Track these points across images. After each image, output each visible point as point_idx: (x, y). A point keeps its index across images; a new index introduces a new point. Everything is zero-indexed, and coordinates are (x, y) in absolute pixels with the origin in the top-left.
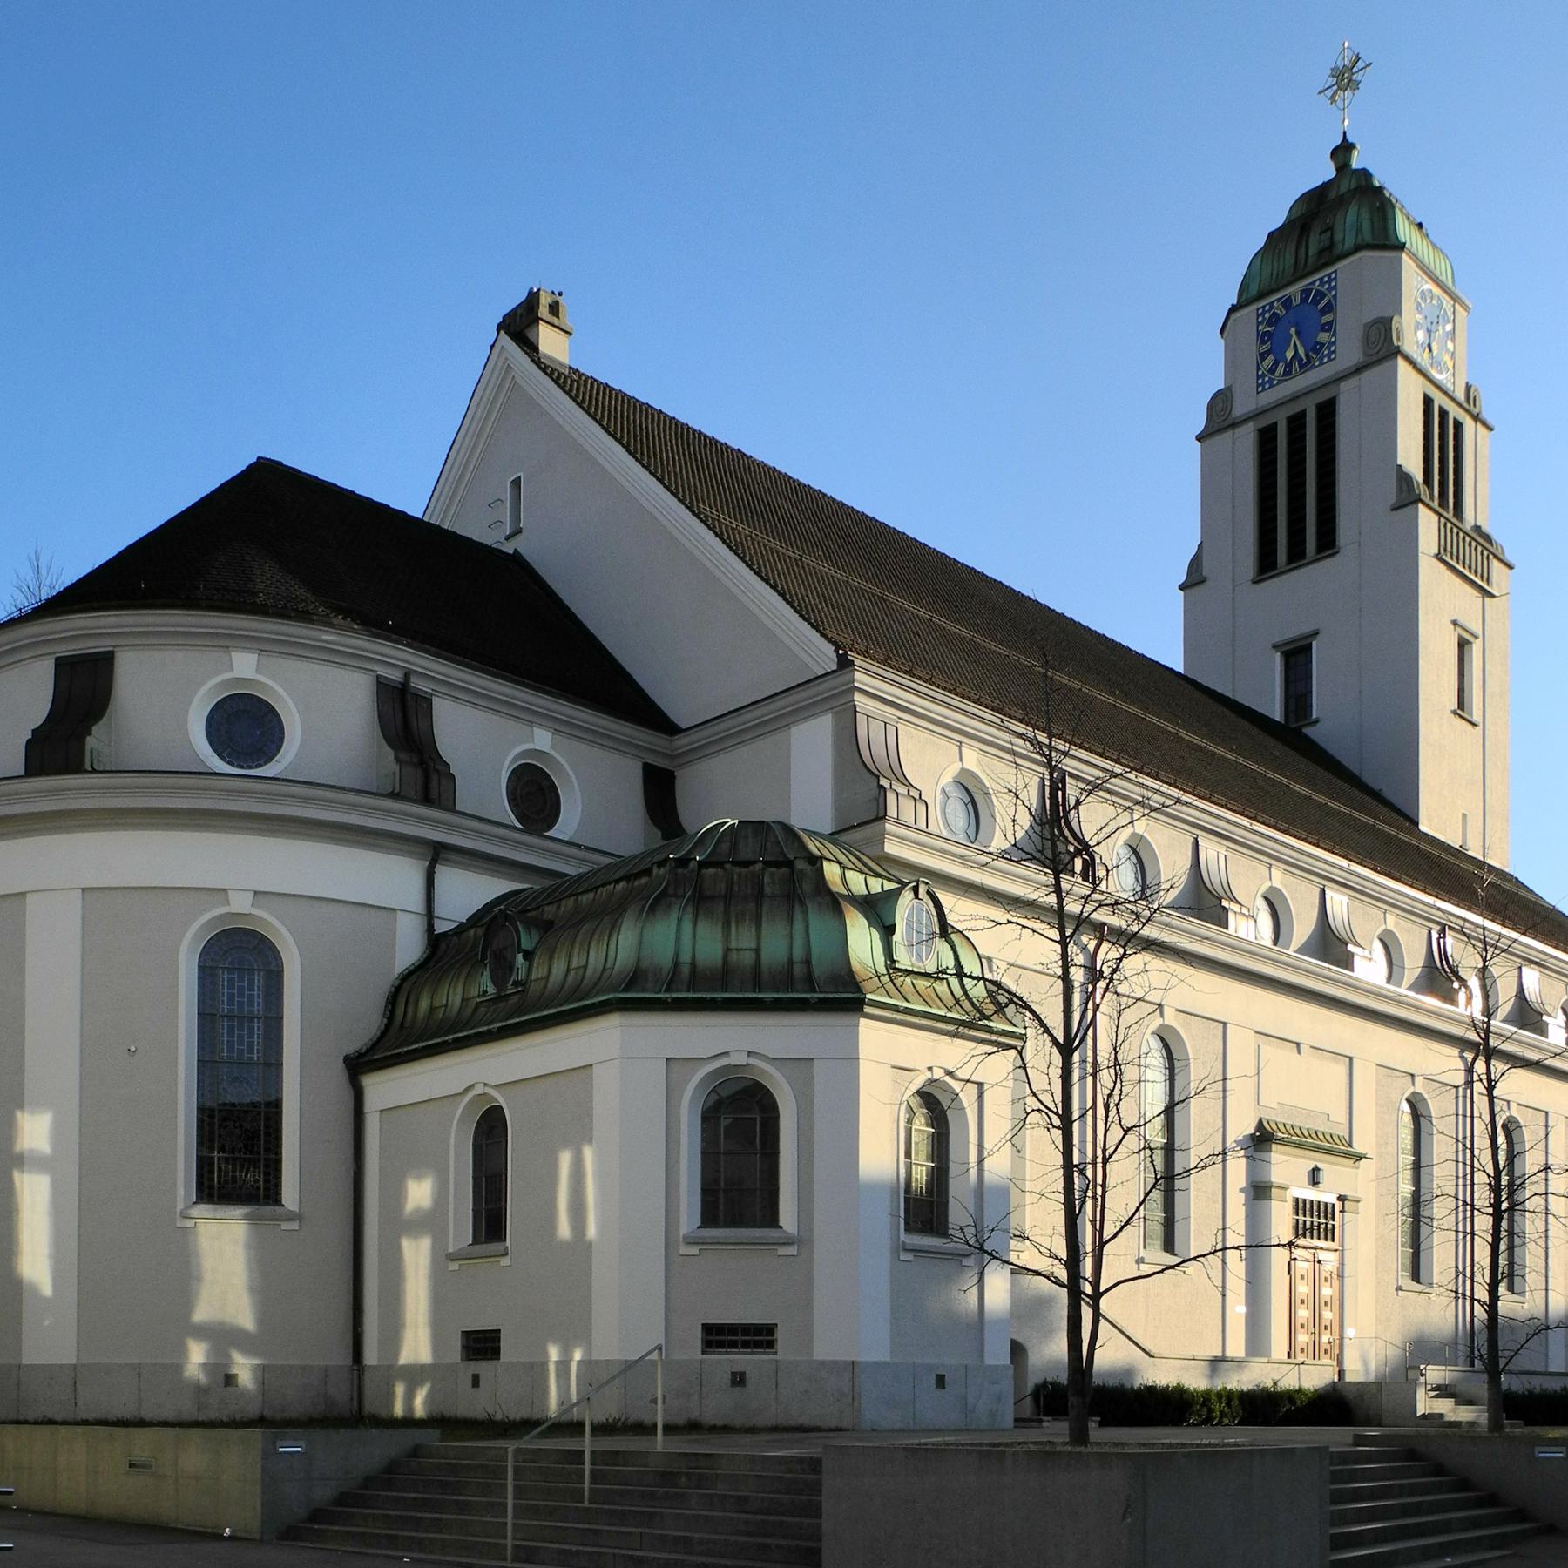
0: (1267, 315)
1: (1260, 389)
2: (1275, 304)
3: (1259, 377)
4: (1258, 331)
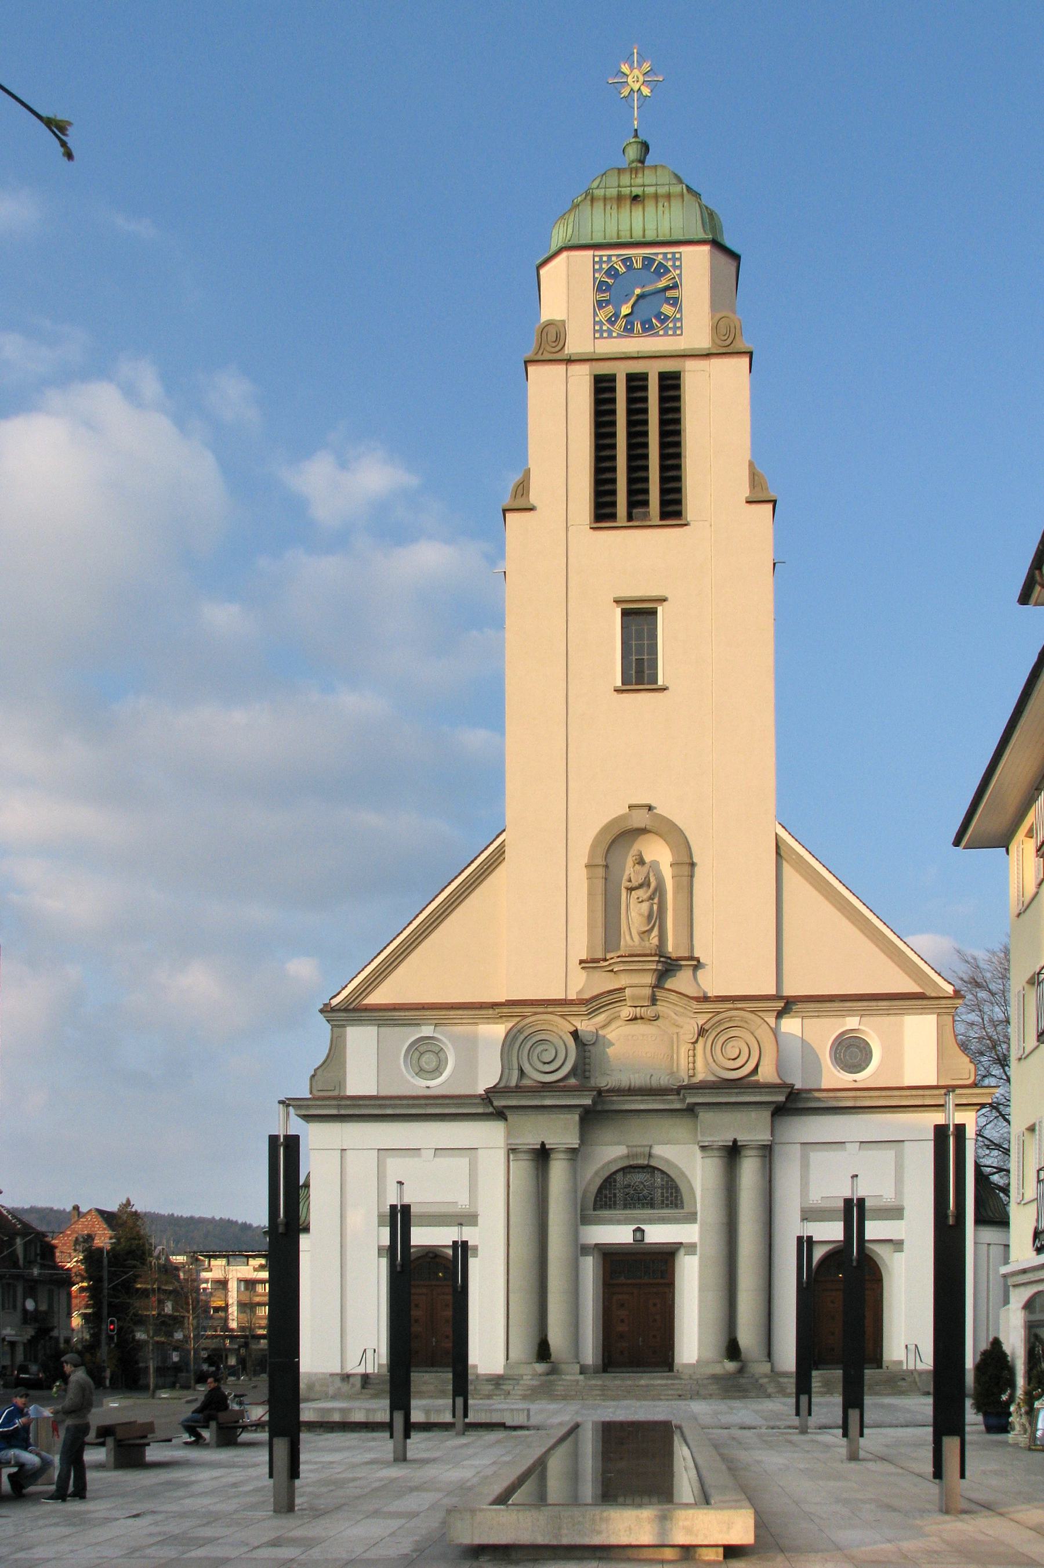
0: (604, 266)
1: (597, 335)
2: (614, 259)
3: (595, 323)
4: (595, 279)
